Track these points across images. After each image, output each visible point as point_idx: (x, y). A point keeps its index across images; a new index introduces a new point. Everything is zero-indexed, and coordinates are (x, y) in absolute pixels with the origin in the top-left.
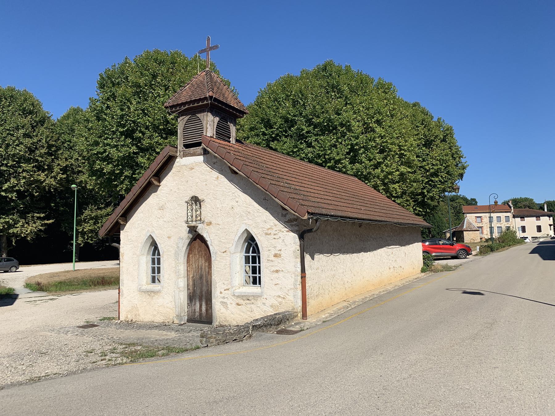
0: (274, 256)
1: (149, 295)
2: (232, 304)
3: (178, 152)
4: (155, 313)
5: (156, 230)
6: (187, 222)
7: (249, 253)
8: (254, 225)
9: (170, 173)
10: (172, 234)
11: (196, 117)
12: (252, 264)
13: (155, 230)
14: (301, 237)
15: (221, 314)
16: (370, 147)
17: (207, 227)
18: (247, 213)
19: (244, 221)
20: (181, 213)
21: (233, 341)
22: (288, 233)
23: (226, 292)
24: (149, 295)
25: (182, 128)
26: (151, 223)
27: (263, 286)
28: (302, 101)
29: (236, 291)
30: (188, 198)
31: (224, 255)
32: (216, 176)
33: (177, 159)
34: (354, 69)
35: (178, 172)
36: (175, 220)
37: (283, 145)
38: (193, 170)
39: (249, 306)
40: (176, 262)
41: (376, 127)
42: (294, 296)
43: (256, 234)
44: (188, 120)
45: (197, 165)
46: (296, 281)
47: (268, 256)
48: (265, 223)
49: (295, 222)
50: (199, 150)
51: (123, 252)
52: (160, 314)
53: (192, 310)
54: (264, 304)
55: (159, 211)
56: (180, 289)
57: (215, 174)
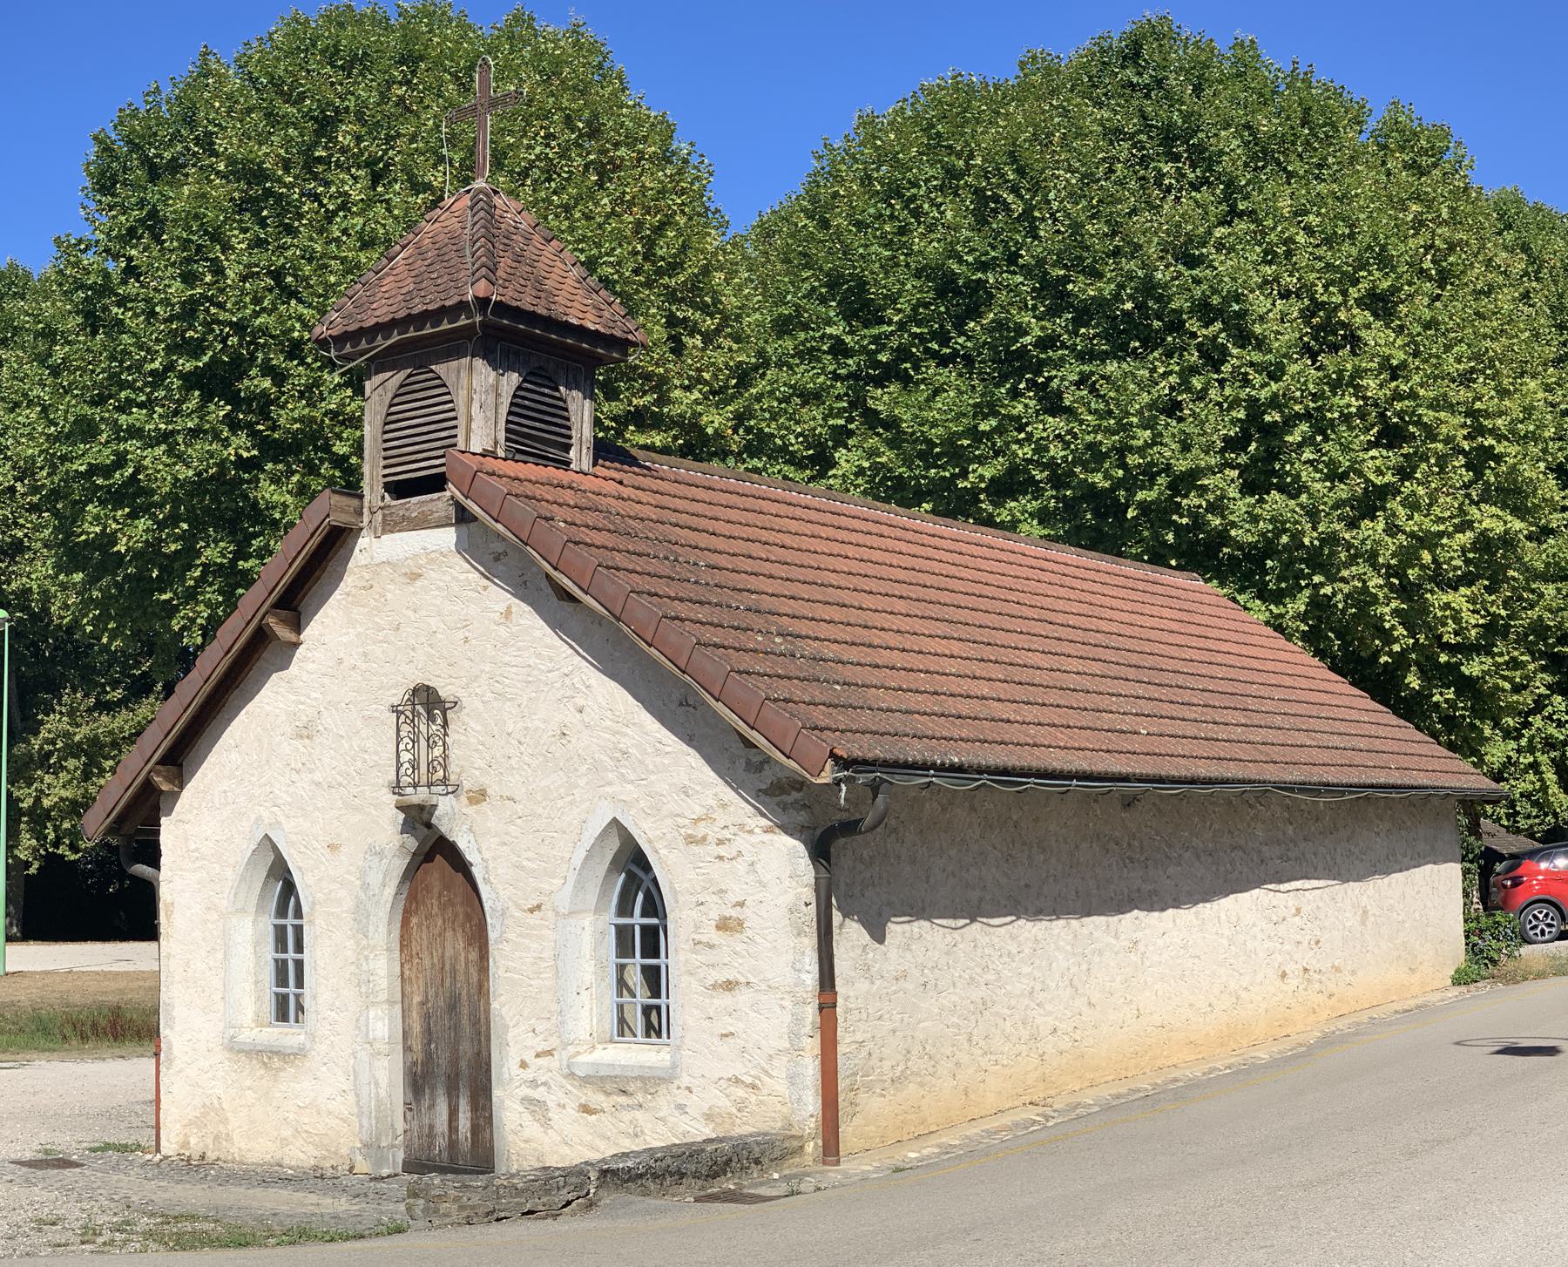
0: (718, 928)
1: (265, 1064)
3: (366, 511)
8: (642, 804)
11: (431, 375)
12: (642, 957)
13: (282, 819)
14: (820, 852)
15: (522, 1146)
16: (1336, 415)
17: (471, 810)
18: (618, 755)
20: (377, 753)
21: (523, 1214)
22: (769, 836)
23: (540, 1061)
24: (265, 1064)
28: (1021, 197)
29: (581, 1059)
30: (398, 695)
31: (532, 922)
32: (502, 607)
33: (360, 540)
37: (927, 400)
38: (418, 583)
39: (626, 1116)
40: (358, 944)
42: (792, 1079)
43: (650, 842)
44: (402, 386)
46: (798, 1020)
47: (697, 927)
48: (683, 796)
49: (795, 795)
50: (440, 504)
52: (304, 1135)
53: (421, 1127)
54: (681, 1108)
55: (296, 743)
56: (377, 1045)
57: (499, 598)
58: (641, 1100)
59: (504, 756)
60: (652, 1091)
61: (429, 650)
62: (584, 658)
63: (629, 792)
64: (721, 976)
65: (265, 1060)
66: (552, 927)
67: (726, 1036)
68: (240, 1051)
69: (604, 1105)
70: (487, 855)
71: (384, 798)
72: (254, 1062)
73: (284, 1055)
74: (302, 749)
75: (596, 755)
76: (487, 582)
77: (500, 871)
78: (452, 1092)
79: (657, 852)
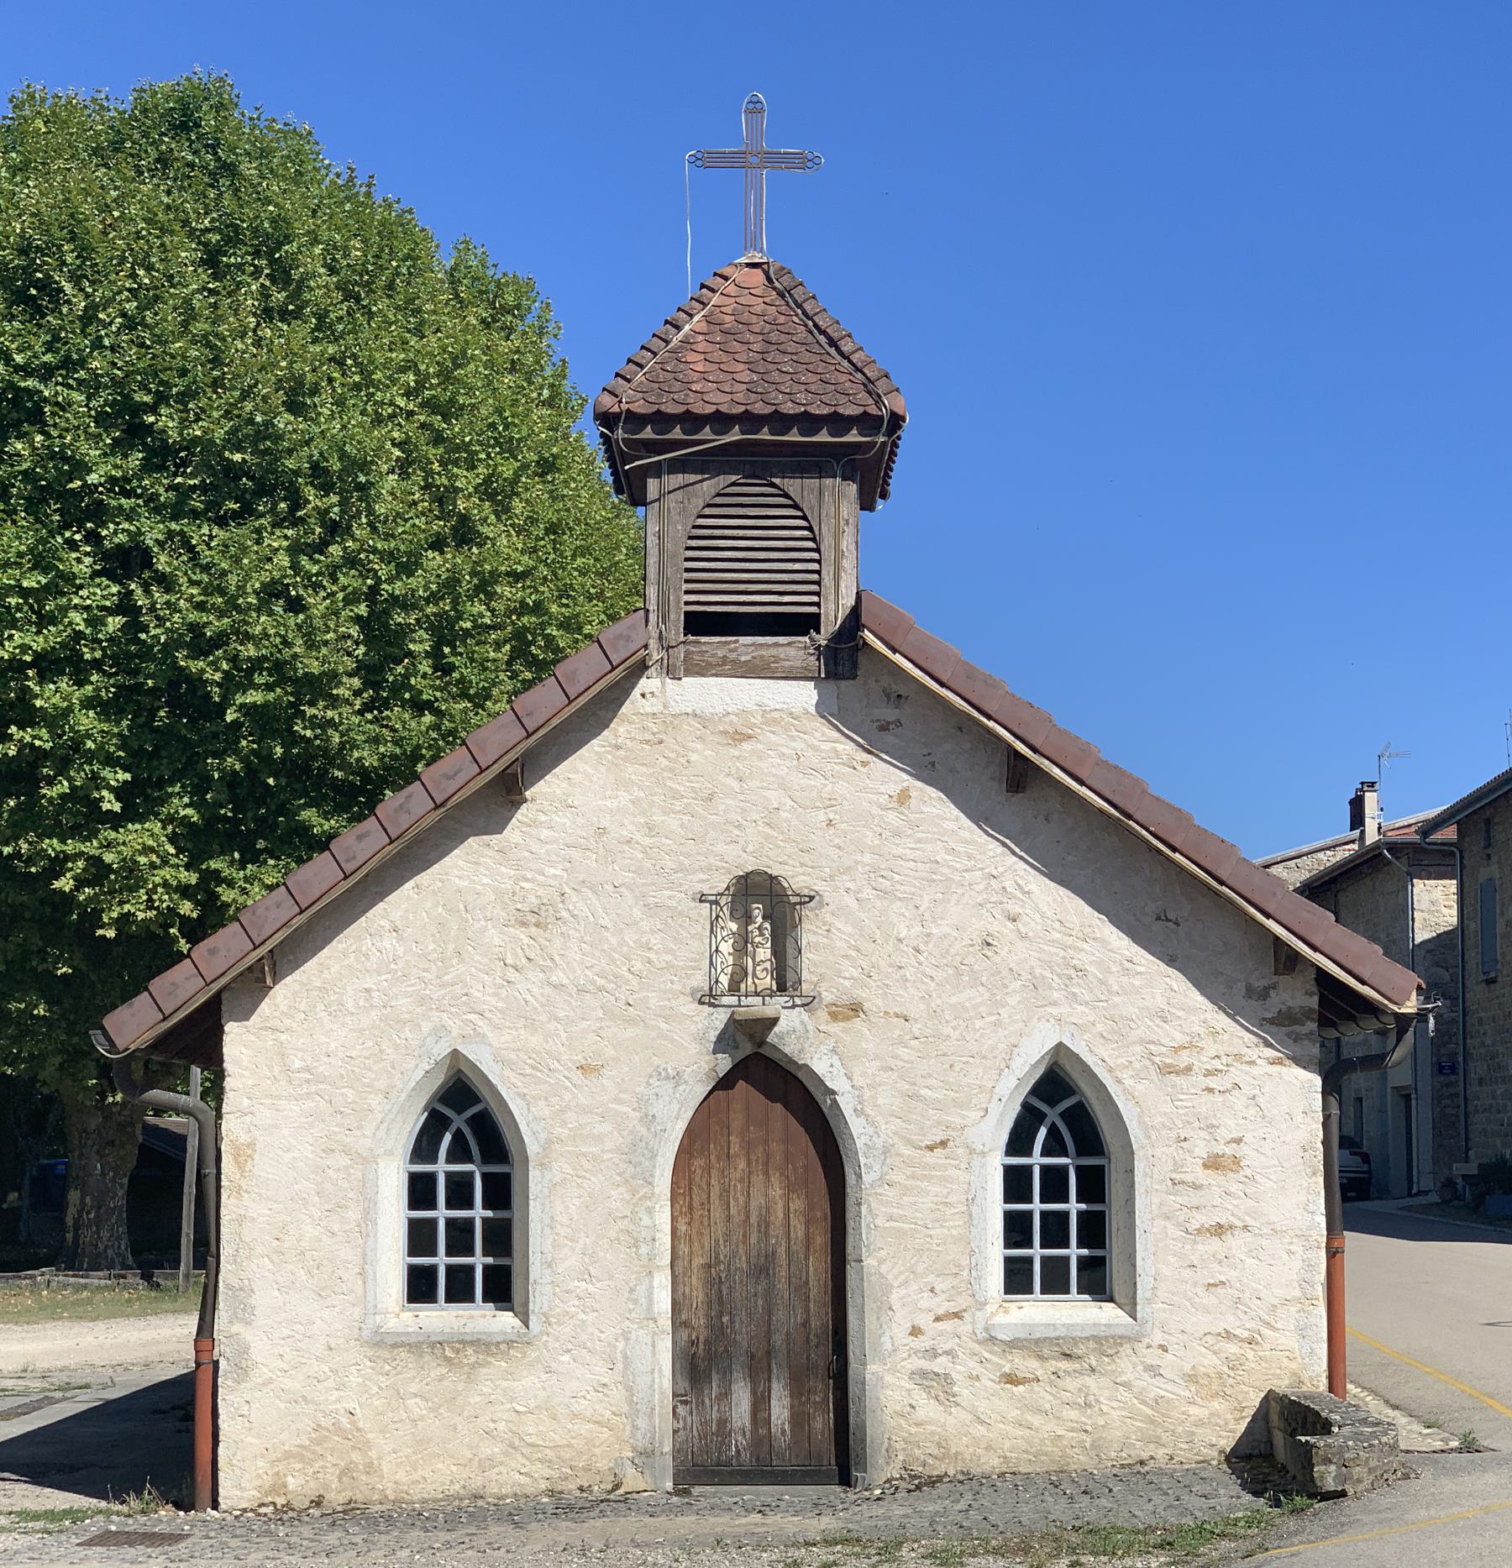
0: (1206, 1166)
2: (978, 1378)
4: (491, 1449)
5: (497, 1027)
6: (711, 995)
7: (1028, 1153)
8: (1100, 1028)
9: (595, 742)
10: (611, 1052)
15: (913, 1430)
16: (468, 625)
17: (835, 1028)
18: (1072, 972)
19: (1049, 1009)
22: (1277, 1068)
23: (941, 1325)
25: (680, 529)
26: (458, 989)
27: (1148, 1295)
29: (1000, 1319)
30: (720, 882)
32: (894, 789)
33: (643, 681)
36: (627, 982)
38: (746, 746)
39: (1071, 1383)
40: (634, 1192)
42: (1302, 1332)
43: (1110, 1070)
45: (776, 722)
46: (1311, 1267)
48: (1158, 1021)
50: (792, 652)
51: (244, 1138)
53: (705, 1423)
54: (1154, 1371)
55: (521, 934)
58: (1094, 1363)
60: (1110, 1352)
61: (767, 830)
62: (1021, 858)
63: (1081, 1013)
64: (1209, 1219)
65: (449, 1353)
66: (963, 1166)
67: (1215, 1285)
68: (384, 1344)
70: (859, 1081)
71: (683, 1010)
72: (427, 1358)
73: (487, 1345)
74: (526, 940)
75: (1038, 971)
77: (880, 1101)
78: (758, 1372)
79: (1119, 1081)
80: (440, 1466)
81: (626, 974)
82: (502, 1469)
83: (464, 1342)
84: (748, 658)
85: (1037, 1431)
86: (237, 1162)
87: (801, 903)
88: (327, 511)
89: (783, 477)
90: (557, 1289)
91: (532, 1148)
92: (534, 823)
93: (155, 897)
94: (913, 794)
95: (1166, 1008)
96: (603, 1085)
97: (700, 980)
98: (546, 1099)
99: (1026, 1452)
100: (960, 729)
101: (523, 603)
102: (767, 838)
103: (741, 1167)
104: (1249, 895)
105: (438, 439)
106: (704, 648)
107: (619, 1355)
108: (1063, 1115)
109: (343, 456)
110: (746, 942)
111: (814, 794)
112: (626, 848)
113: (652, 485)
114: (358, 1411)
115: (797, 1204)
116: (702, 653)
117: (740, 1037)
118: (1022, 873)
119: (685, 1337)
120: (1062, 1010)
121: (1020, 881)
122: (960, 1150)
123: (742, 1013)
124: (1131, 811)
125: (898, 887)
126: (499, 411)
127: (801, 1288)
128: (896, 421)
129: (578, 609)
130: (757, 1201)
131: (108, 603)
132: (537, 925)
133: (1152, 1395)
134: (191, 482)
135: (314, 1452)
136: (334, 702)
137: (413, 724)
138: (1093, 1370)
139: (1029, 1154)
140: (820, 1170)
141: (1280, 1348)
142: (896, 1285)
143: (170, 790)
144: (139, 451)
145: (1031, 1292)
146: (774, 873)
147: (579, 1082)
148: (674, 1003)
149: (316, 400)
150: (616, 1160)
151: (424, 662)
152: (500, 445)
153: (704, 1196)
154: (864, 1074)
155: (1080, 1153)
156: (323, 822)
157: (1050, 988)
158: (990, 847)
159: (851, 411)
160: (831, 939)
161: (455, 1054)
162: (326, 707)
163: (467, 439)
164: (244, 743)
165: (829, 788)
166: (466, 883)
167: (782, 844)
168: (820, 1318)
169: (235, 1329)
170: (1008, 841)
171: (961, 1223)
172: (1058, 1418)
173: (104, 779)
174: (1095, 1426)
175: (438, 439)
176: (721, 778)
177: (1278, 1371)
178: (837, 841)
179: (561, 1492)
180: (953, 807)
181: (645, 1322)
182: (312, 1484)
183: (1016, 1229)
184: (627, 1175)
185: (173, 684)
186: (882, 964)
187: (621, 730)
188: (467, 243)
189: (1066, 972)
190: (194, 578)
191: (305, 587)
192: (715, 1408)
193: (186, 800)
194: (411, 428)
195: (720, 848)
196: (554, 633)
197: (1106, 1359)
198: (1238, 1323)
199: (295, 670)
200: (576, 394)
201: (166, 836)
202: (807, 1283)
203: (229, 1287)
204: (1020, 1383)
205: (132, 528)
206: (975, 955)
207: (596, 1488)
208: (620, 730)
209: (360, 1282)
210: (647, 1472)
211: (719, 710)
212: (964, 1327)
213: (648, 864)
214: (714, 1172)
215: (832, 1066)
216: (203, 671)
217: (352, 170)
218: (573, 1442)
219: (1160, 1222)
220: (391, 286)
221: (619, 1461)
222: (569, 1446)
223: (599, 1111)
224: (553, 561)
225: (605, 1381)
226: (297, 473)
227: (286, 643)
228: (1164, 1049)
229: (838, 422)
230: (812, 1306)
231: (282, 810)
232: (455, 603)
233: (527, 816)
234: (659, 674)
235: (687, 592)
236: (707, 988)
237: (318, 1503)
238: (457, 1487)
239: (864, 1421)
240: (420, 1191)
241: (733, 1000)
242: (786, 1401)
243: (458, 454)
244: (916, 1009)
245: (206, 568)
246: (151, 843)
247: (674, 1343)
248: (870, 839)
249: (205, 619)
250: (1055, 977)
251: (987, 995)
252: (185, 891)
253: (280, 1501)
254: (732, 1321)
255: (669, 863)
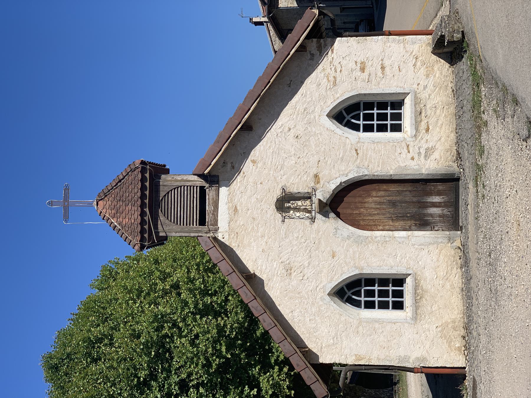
0: (364, 72)
1: (420, 298)
4: (448, 285)
6: (312, 219)
7: (359, 125)
8: (322, 104)
12: (374, 121)
13: (322, 285)
15: (443, 159)
16: (202, 286)
17: (322, 182)
18: (305, 112)
19: (317, 119)
20: (299, 230)
22: (334, 51)
23: (411, 151)
24: (420, 298)
25: (175, 227)
26: (310, 293)
27: (402, 89)
29: (409, 133)
30: (279, 216)
31: (361, 154)
32: (251, 164)
33: (219, 238)
34: (67, 325)
35: (237, 237)
36: (308, 243)
38: (238, 208)
39: (429, 112)
40: (370, 242)
41: (172, 281)
42: (414, 43)
43: (335, 101)
46: (394, 40)
48: (320, 87)
50: (211, 194)
51: (354, 358)
53: (440, 221)
54: (425, 87)
55: (294, 274)
57: (248, 167)
58: (423, 105)
59: (303, 166)
60: (419, 100)
61: (263, 202)
63: (318, 110)
64: (380, 71)
65: (419, 298)
66: (363, 145)
68: (416, 317)
69: (426, 122)
70: (338, 175)
73: (416, 286)
74: (295, 273)
75: (305, 122)
76: (242, 173)
77: (344, 169)
79: (338, 98)
80: (453, 301)
81: (306, 244)
82: (454, 282)
83: (415, 293)
84: (212, 207)
85: (443, 122)
86: (361, 360)
87: (285, 192)
88: (169, 327)
89: (160, 197)
90: (399, 265)
91: (357, 272)
92: (261, 271)
93: (282, 379)
94: (253, 159)
95: (316, 84)
96: (338, 251)
97: (308, 222)
98: (342, 268)
99: (450, 126)
100: (234, 145)
101: (196, 270)
102: (265, 202)
103: (363, 210)
104: (283, 60)
105: (148, 294)
106: (210, 220)
107: (420, 247)
108: (348, 115)
109: (153, 322)
110: (296, 208)
111: (252, 188)
112: (268, 243)
113: (161, 234)
114: (436, 325)
115: (374, 194)
116: (211, 221)
117: (324, 211)
118: (276, 126)
119: (414, 227)
120: (317, 115)
121: (279, 127)
122: (358, 145)
123: (317, 210)
124: (257, 95)
125: (280, 163)
126: (140, 276)
127: (399, 193)
128: (143, 162)
129: (198, 253)
130: (373, 206)
131: (196, 392)
132: (291, 270)
133: (433, 88)
134: (160, 367)
135: (448, 338)
136: (225, 325)
137: (232, 302)
138: (425, 105)
139: (359, 125)
140: (364, 187)
141: (418, 50)
142: (398, 164)
143: (251, 374)
144: (151, 382)
145: (401, 124)
146: (276, 200)
147: (337, 258)
148: (314, 230)
149: (137, 330)
150: (361, 247)
151: (214, 299)
152: (150, 276)
153: (372, 221)
154: (336, 174)
155: (359, 110)
156: (260, 329)
157: (310, 118)
158: (268, 136)
159: (140, 176)
160: (295, 183)
161: (329, 294)
162: (227, 328)
163: (148, 285)
164: (237, 352)
165: (251, 184)
166: (278, 291)
167: (267, 197)
168: (408, 187)
169: (411, 361)
170: (267, 131)
171: (380, 145)
172: (439, 116)
173: (247, 394)
174: (442, 105)
175: (148, 294)
176: (248, 215)
177: (426, 50)
178: (266, 181)
179: (461, 265)
180: (256, 147)
181: (409, 239)
182: (458, 339)
183: (382, 128)
184: (365, 244)
185: (220, 373)
186: (303, 168)
187: (233, 245)
188: (91, 286)
189: (305, 114)
190: (188, 366)
191: (191, 334)
192: (435, 218)
193: (254, 369)
194: (145, 302)
195: (268, 216)
196: (205, 260)
197: (421, 102)
198: (411, 62)
199: (216, 337)
200: (135, 253)
201: (264, 375)
202: (398, 191)
203: (399, 363)
204: (429, 127)
205: (174, 385)
206: (300, 141)
207: (460, 254)
208: (233, 245)
209: (397, 324)
210: (455, 239)
211: (228, 216)
212: (412, 144)
213: (273, 237)
214: (365, 218)
215: (333, 183)
216: (216, 364)
217: (69, 319)
218: (445, 261)
219: (380, 86)
220: (103, 308)
221: (452, 247)
222: (447, 262)
223: (346, 252)
224: (184, 260)
225: (427, 251)
226: (158, 336)
227: (208, 339)
228: (329, 85)
229: (143, 180)
230: (405, 189)
231: (257, 341)
232: (196, 289)
233: (259, 273)
234: (217, 233)
235: (193, 225)
236: (310, 220)
237: (464, 337)
238: (459, 296)
239: (440, 174)
240: (370, 305)
241: (313, 212)
242: (434, 197)
243: (153, 288)
244: (316, 158)
245: (186, 363)
246: (266, 380)
247: (416, 230)
248: (266, 171)
249: (201, 363)
250: (307, 117)
251: (312, 137)
252: (281, 370)
253: (463, 348)
254: (409, 213)
255: (273, 231)
